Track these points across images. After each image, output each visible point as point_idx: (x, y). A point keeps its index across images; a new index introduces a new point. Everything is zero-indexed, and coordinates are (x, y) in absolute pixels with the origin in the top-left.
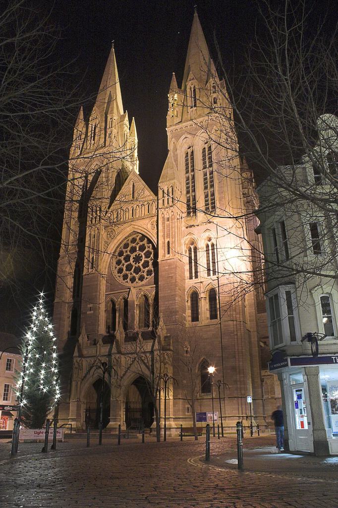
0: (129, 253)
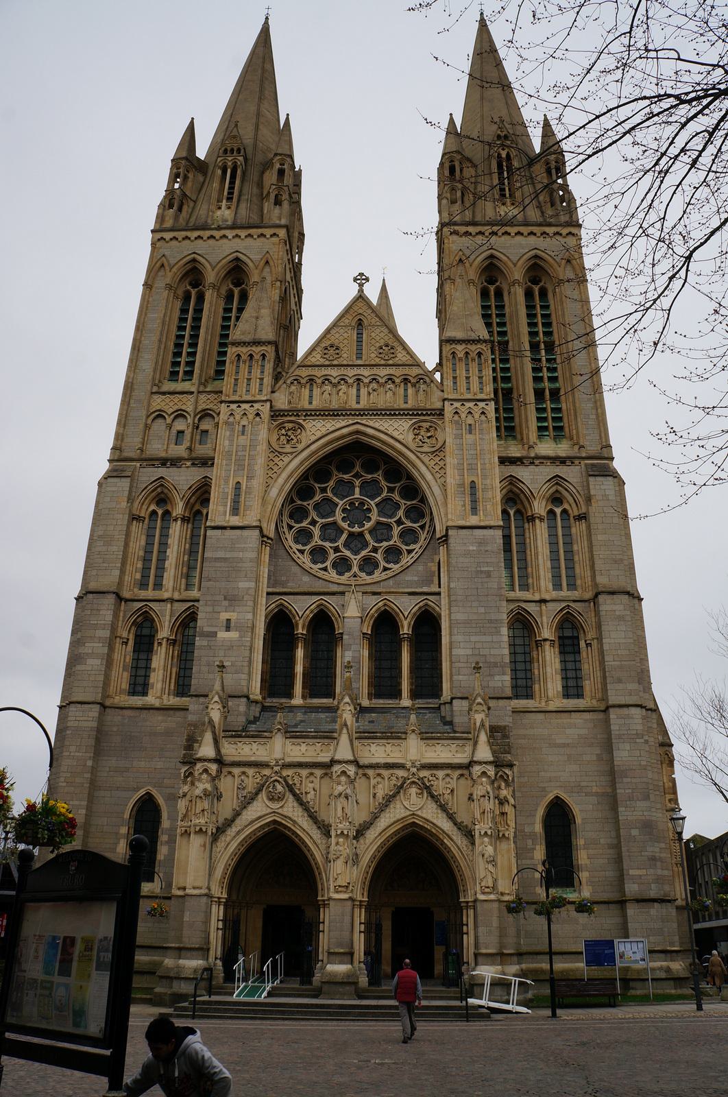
0: (330, 494)
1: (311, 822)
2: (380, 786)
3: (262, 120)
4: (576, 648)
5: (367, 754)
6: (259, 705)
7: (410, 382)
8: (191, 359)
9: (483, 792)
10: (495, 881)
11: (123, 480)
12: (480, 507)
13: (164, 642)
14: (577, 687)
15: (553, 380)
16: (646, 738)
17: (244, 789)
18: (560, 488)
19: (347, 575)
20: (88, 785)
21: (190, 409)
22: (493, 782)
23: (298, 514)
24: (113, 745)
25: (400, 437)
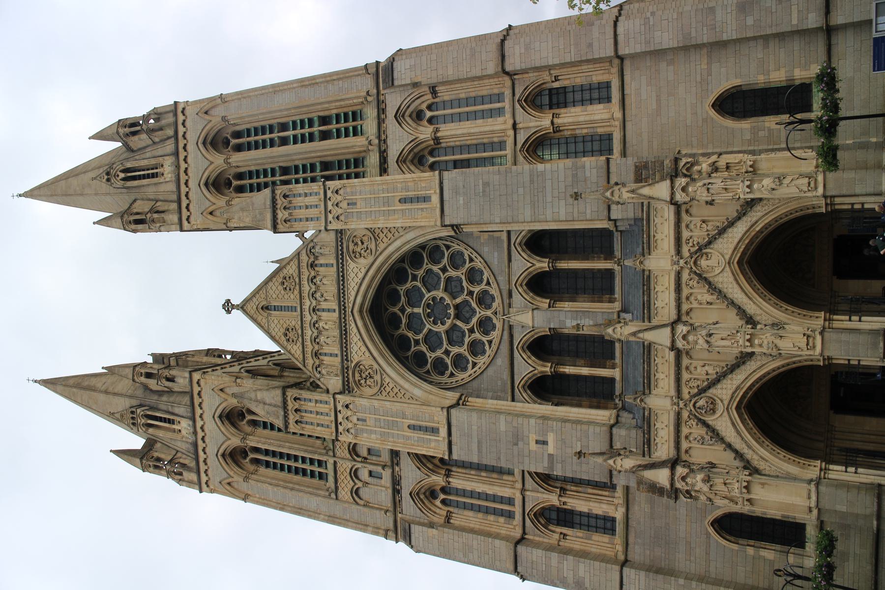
0: (420, 337)
1: (737, 371)
2: (699, 297)
3: (110, 389)
4: (561, 91)
5: (666, 310)
6: (621, 413)
7: (314, 262)
8: (308, 461)
9: (704, 190)
10: (802, 176)
11: (412, 531)
12: (422, 193)
13: (563, 499)
14: (599, 88)
15: (311, 123)
16: (648, 14)
17: (703, 438)
18: (407, 113)
19: (495, 321)
20: (704, 585)
21: (349, 464)
22: (693, 180)
23: (439, 366)
24: (663, 555)
25: (364, 271)
